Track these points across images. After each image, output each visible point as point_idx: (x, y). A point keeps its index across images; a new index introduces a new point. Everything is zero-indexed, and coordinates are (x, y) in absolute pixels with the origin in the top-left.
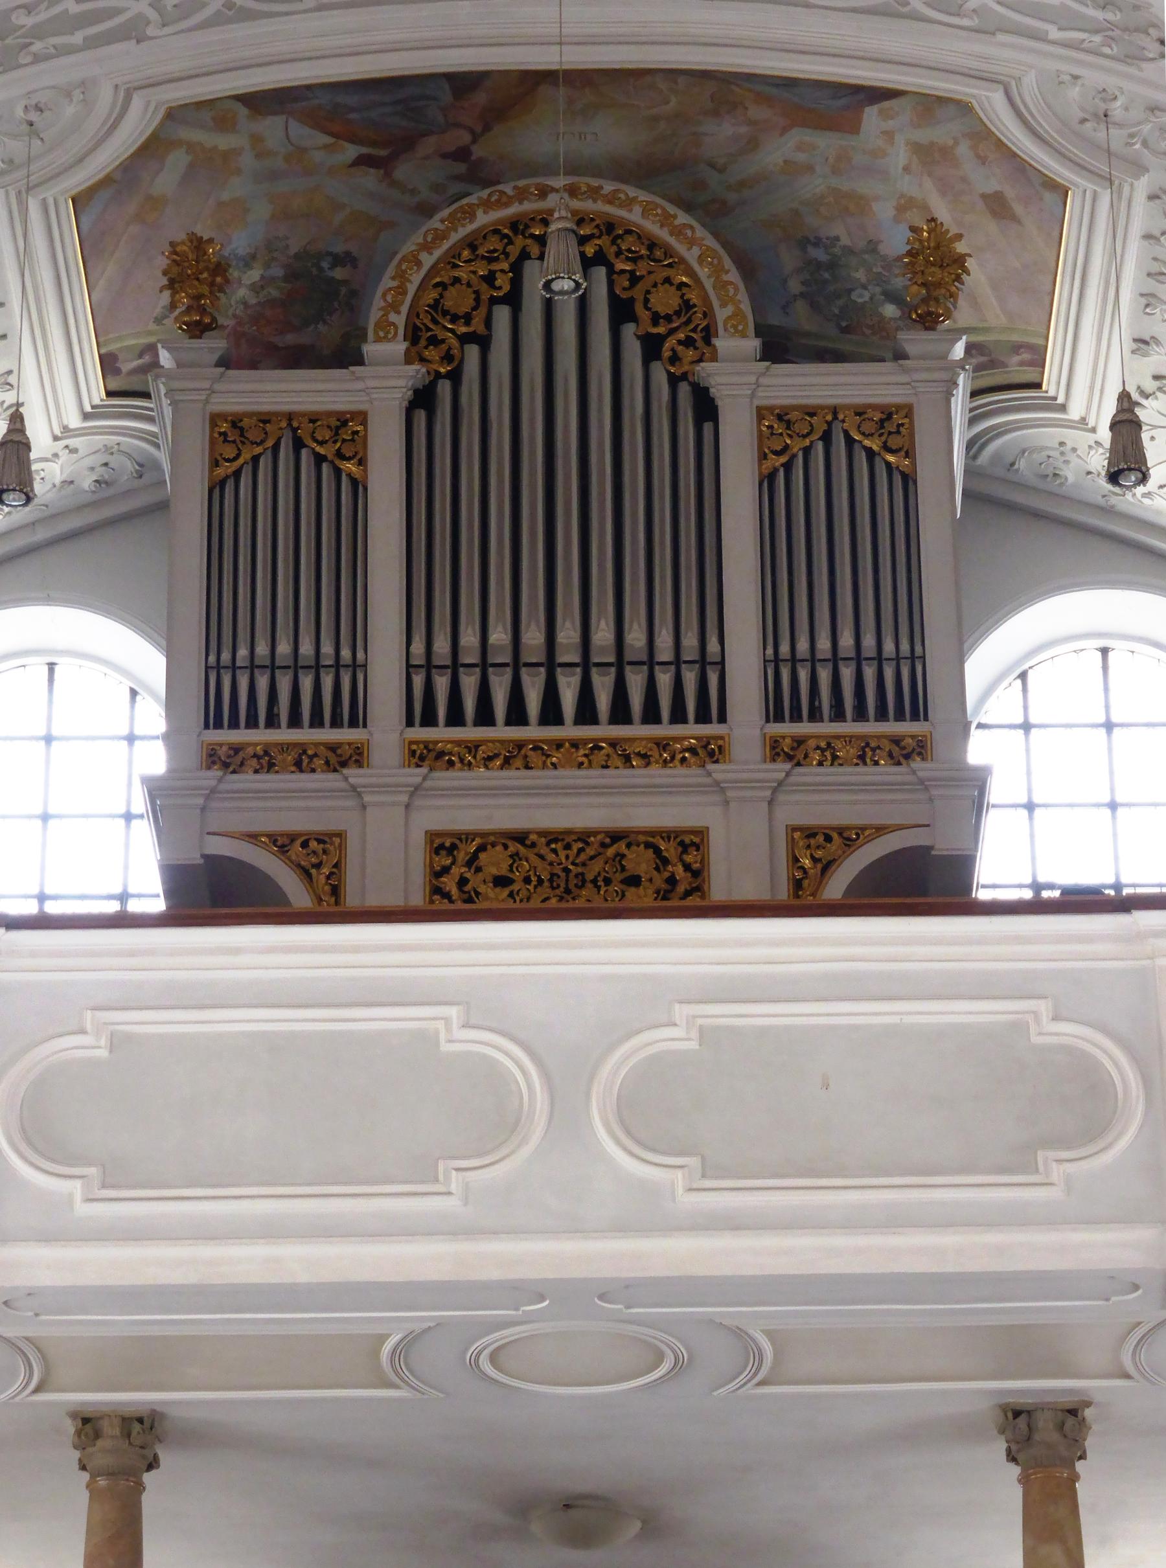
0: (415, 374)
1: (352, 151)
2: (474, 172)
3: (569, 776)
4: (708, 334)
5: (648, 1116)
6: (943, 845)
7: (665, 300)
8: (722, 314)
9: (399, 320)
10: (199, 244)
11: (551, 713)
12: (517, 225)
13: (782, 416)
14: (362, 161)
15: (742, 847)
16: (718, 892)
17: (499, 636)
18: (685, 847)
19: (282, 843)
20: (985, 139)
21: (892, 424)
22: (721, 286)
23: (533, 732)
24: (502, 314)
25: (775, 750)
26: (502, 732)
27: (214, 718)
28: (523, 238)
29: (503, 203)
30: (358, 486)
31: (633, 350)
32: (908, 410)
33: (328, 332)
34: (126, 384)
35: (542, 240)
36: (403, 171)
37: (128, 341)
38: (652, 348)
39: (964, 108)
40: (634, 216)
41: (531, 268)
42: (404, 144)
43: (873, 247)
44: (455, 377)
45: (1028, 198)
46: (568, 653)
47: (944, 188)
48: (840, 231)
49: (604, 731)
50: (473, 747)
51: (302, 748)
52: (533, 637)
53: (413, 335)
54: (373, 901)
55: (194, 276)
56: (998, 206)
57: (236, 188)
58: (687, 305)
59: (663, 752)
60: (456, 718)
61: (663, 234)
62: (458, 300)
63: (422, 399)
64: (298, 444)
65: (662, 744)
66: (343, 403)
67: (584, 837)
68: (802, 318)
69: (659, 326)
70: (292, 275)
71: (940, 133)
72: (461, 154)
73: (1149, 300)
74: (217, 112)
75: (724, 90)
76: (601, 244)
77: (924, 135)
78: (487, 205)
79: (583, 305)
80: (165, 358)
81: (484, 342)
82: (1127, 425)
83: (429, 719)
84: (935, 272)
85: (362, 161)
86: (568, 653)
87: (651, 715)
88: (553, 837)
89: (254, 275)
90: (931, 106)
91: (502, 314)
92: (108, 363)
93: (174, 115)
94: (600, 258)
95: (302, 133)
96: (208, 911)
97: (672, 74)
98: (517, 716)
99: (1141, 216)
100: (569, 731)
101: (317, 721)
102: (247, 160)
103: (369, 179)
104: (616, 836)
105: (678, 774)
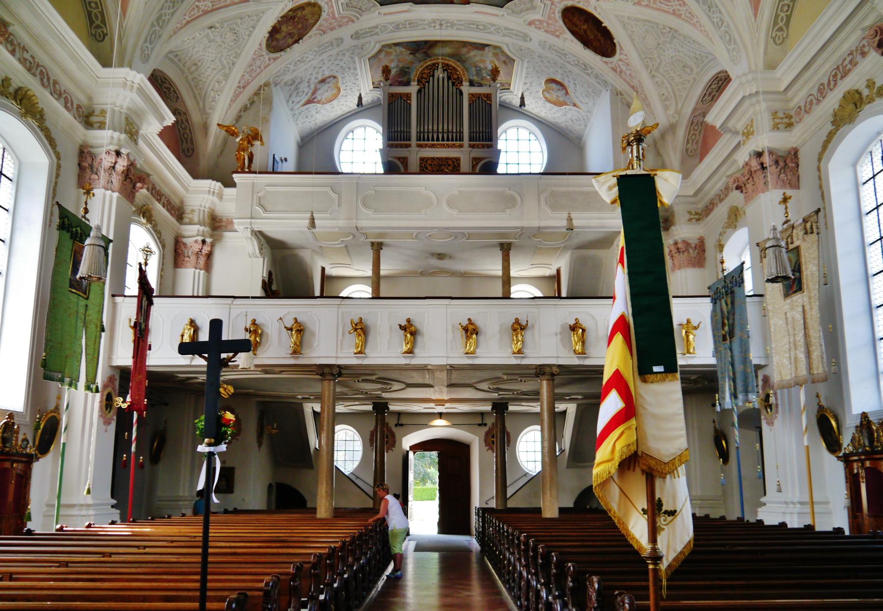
0: (418, 87)
2: (427, 56)
3: (440, 149)
5: (451, 203)
6: (494, 160)
7: (455, 76)
10: (387, 66)
12: (434, 64)
13: (472, 95)
15: (465, 165)
16: (462, 170)
17: (430, 127)
19: (399, 158)
20: (503, 52)
21: (488, 96)
23: (435, 142)
25: (470, 146)
28: (434, 67)
30: (410, 104)
33: (405, 79)
34: (376, 87)
36: (417, 55)
37: (376, 80)
38: (453, 84)
39: (500, 48)
40: (451, 63)
45: (509, 61)
46: (440, 130)
48: (482, 65)
49: (445, 142)
52: (435, 128)
53: (418, 81)
54: (412, 171)
55: (386, 71)
56: (505, 62)
57: (392, 57)
59: (453, 146)
60: (424, 140)
62: (424, 76)
63: (419, 91)
68: (475, 78)
69: (455, 80)
71: (497, 51)
72: (425, 53)
73: (526, 77)
75: (465, 44)
76: (446, 67)
79: (443, 78)
81: (429, 82)
82: (522, 98)
84: (495, 73)
86: (440, 130)
87: (452, 140)
88: (438, 158)
90: (495, 47)
92: (373, 83)
93: (383, 46)
97: (457, 41)
98: (433, 140)
99: (526, 65)
100: (440, 142)
103: (412, 56)
104: (447, 158)
105: (456, 149)
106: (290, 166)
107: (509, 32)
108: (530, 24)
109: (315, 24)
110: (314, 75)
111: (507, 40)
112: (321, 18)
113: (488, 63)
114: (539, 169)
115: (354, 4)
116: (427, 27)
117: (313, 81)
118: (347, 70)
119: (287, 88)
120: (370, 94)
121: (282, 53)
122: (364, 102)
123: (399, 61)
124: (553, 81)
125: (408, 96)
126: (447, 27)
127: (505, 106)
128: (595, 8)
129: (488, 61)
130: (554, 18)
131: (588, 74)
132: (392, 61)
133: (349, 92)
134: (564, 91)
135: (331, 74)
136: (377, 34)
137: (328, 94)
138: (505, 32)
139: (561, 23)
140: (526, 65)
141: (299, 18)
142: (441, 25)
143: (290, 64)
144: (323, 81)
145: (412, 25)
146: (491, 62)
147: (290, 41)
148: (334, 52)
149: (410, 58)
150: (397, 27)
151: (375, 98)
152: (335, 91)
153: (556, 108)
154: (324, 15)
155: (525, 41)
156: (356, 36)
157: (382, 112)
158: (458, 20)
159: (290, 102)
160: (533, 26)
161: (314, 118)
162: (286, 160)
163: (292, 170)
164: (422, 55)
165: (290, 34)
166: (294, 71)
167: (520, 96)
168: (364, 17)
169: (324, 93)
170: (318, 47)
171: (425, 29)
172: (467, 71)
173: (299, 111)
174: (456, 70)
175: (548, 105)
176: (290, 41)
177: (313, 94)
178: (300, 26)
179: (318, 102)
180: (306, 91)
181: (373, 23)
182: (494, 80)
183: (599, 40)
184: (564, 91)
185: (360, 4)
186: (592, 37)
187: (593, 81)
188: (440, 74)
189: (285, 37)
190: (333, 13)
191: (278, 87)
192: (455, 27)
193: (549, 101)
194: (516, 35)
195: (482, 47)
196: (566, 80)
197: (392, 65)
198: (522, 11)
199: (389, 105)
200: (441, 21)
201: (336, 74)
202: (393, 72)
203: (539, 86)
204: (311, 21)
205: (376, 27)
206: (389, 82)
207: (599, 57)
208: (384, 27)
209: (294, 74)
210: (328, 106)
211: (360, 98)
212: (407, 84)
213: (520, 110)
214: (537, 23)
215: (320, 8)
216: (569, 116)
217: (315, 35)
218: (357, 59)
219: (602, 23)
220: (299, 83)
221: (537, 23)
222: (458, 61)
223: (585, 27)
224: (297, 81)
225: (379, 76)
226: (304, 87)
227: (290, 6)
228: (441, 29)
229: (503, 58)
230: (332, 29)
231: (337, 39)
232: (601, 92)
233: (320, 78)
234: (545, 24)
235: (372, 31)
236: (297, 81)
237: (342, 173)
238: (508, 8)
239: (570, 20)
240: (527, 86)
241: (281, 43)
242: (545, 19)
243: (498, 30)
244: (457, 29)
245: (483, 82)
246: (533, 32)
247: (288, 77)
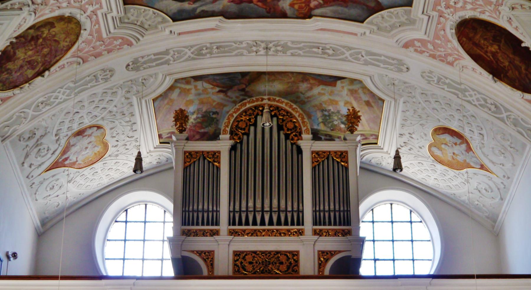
0: (232, 142)
1: (218, 89)
2: (246, 94)
4: (300, 133)
7: (290, 125)
8: (304, 129)
9: (228, 129)
10: (182, 111)
11: (263, 223)
12: (256, 107)
13: (317, 153)
14: (220, 91)
15: (307, 262)
16: (302, 272)
17: (251, 204)
18: (294, 255)
19: (200, 253)
20: (364, 88)
21: (343, 155)
22: (303, 122)
23: (258, 227)
24: (252, 128)
25: (315, 233)
26: (251, 227)
27: (184, 223)
28: (257, 111)
29: (253, 102)
30: (218, 168)
31: (282, 136)
32: (346, 152)
33: (210, 130)
34: (164, 141)
35: (262, 111)
36: (230, 94)
37: (165, 133)
38: (287, 137)
39: (360, 82)
40: (283, 106)
41: (259, 118)
42: (230, 87)
43: (338, 112)
44: (241, 143)
45: (375, 102)
46: (267, 208)
47: (356, 99)
48: (331, 108)
49: (275, 227)
50: (244, 231)
51: (204, 230)
52: (259, 205)
53: (231, 133)
54: (220, 274)
55: (181, 118)
56: (368, 103)
57: (191, 97)
58: (295, 127)
59: (288, 233)
60: (240, 224)
61: (290, 110)
62: (241, 125)
63: (233, 148)
64: (204, 158)
65: (289, 231)
66: (214, 149)
67: (270, 252)
68: (322, 127)
69: (289, 130)
70: (203, 117)
71: (355, 87)
72: (243, 90)
73: (403, 126)
74: (186, 80)
75: (305, 77)
76: (275, 112)
77: (351, 87)
78: (249, 102)
79: (271, 129)
80: (174, 138)
81: (248, 135)
82: (397, 158)
83: (234, 224)
84: (353, 119)
85: (220, 91)
86: (267, 208)
87: (286, 224)
88: (263, 252)
89: (195, 116)
90: (353, 81)
91: (252, 128)
92: (160, 136)
93: (176, 81)
94: (275, 115)
95: (206, 85)
96: (183, 276)
97: (292, 73)
98: (255, 223)
99: (401, 106)
100: (267, 227)
101: (208, 224)
102: (193, 91)
103: (221, 95)
104: (277, 252)
105: (292, 238)
106: (21, 266)
107: (374, 58)
108: (406, 46)
109: (69, 48)
110: (67, 124)
111: (371, 70)
112: (80, 40)
113: (341, 104)
114: (426, 268)
115: (132, 18)
116: (245, 52)
117: (65, 133)
118: (119, 116)
119: (23, 144)
120: (154, 154)
121: (17, 91)
122: (145, 164)
123: (202, 102)
124: (446, 130)
125: (216, 155)
126: (277, 51)
127: (367, 169)
128: (510, 20)
129: (341, 102)
130: (445, 36)
131: (502, 120)
132: (191, 102)
133: (122, 149)
134: (464, 146)
135: (94, 122)
136: (167, 62)
137: (89, 154)
138: (367, 58)
139: (455, 43)
140: (401, 106)
141: (45, 39)
142: (267, 48)
143: (28, 107)
144: (80, 133)
145: (222, 49)
146: (346, 103)
147: (30, 73)
148: (99, 89)
149: (218, 98)
150: (199, 53)
151: (163, 159)
152: (99, 149)
153: (451, 173)
154: (84, 35)
155: (400, 71)
156: (134, 65)
157: (174, 179)
158: (293, 42)
159: (26, 165)
160: (411, 49)
161: (63, 190)
162: (15, 255)
163: (25, 272)
164: (237, 94)
165: (29, 62)
166: (34, 118)
167: (393, 154)
168: (145, 38)
169: (82, 150)
170: (75, 82)
171: (242, 55)
172: (309, 117)
173: (40, 179)
174: (292, 116)
175: (439, 167)
176: (30, 73)
177: (64, 152)
178: (46, 50)
179: (72, 165)
180: (52, 147)
181: (161, 47)
182: (352, 130)
183: (518, 68)
184: (464, 146)
185: (141, 19)
186: (507, 64)
187: (510, 130)
188: (265, 122)
189: (22, 67)
190: (99, 31)
191: (7, 142)
192: (289, 53)
193: (441, 162)
194: (385, 62)
195: (332, 80)
196: (467, 129)
197: (191, 109)
198: (393, 27)
199: (185, 169)
200: (267, 42)
201: (100, 123)
202: (192, 119)
203: (424, 139)
204: (64, 44)
205: (167, 52)
206: (185, 135)
207: (518, 94)
208: (179, 52)
209: (35, 123)
210: (87, 171)
211: (139, 159)
212: (215, 137)
213: (394, 175)
214: (417, 44)
215: (78, 24)
216: (474, 183)
217: (71, 63)
218: (134, 100)
219: (521, 42)
220: (42, 136)
221: (417, 44)
222: (295, 102)
223: (494, 48)
224: (38, 134)
225: (170, 126)
226: (49, 142)
227: (31, 21)
228: (267, 55)
229: (365, 98)
230: (97, 56)
231: (104, 70)
232: (524, 146)
233: (76, 128)
234: (430, 46)
235: (160, 58)
236: (38, 134)
237: (101, 277)
238: (371, 23)
239: (470, 39)
240: (405, 139)
241: (15, 75)
242: (431, 39)
243: (357, 55)
244: (292, 55)
245: (332, 133)
246: (411, 58)
247: (24, 128)
